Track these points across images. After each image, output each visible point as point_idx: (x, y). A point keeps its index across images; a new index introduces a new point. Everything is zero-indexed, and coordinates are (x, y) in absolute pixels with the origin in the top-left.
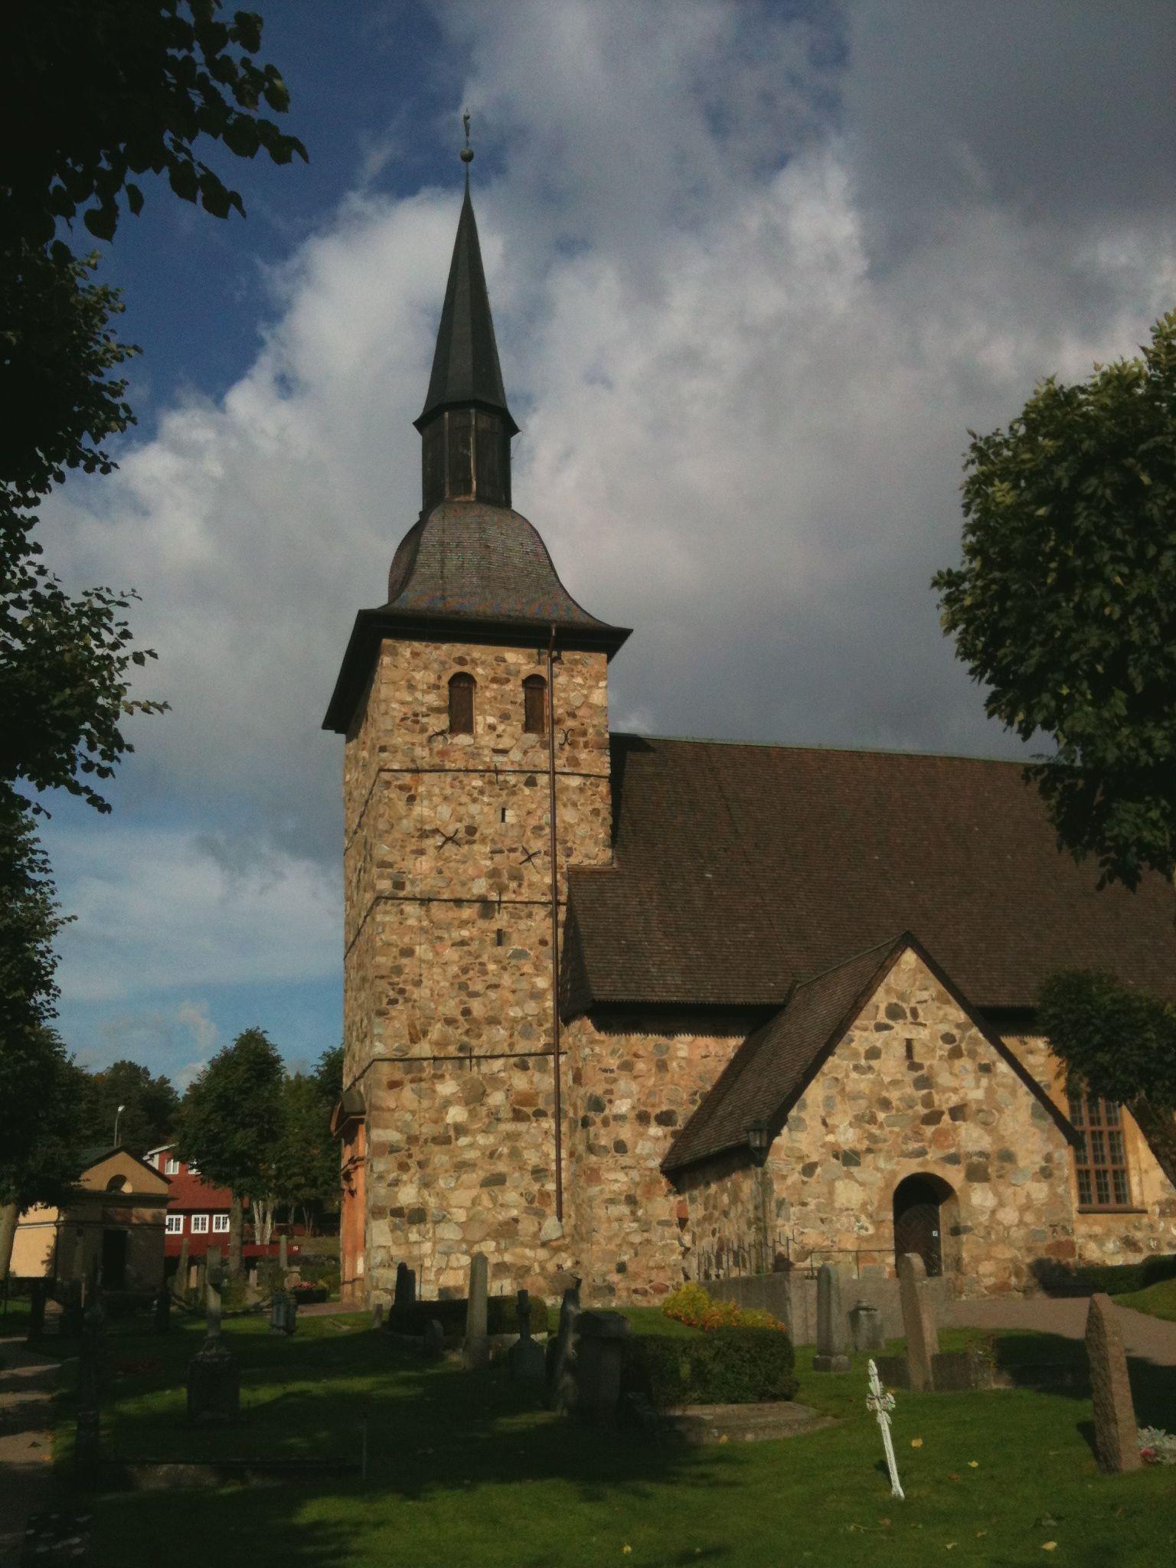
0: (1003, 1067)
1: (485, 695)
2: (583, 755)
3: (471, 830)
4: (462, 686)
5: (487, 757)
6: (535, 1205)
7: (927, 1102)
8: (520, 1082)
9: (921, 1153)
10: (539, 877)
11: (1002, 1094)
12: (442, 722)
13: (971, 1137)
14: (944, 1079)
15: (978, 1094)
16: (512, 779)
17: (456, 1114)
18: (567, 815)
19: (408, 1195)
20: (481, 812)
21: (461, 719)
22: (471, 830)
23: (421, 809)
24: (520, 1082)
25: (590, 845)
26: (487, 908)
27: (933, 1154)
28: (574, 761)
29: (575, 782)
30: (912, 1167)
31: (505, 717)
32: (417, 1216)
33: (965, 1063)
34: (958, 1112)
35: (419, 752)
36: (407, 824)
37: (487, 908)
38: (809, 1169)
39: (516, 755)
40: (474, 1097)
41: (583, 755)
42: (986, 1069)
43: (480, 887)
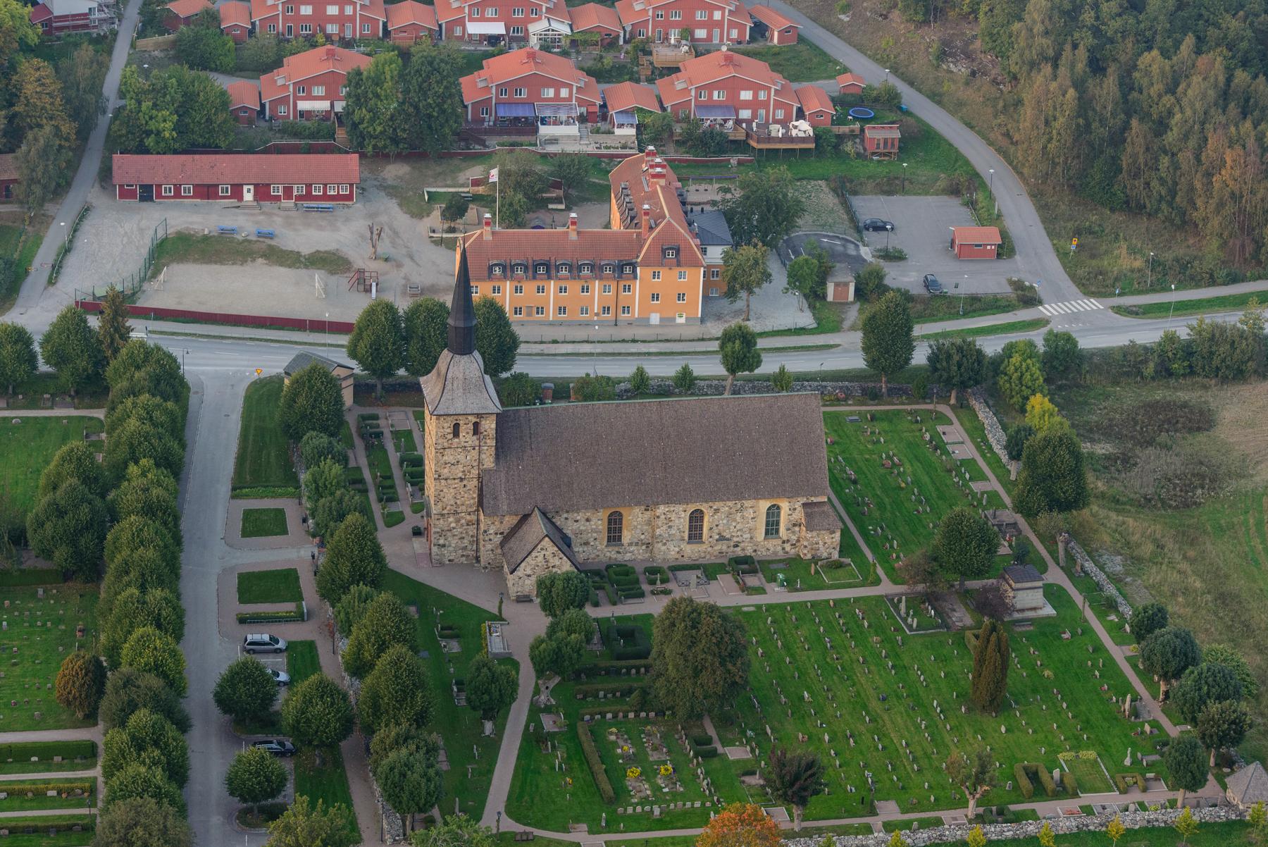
1: (462, 428)
6: (471, 543)
8: (468, 517)
10: (475, 472)
17: (453, 525)
18: (483, 456)
19: (441, 542)
20: (461, 457)
21: (456, 433)
23: (446, 458)
24: (468, 517)
25: (489, 462)
26: (462, 480)
32: (444, 546)
37: (462, 480)
40: (458, 521)
43: (460, 475)
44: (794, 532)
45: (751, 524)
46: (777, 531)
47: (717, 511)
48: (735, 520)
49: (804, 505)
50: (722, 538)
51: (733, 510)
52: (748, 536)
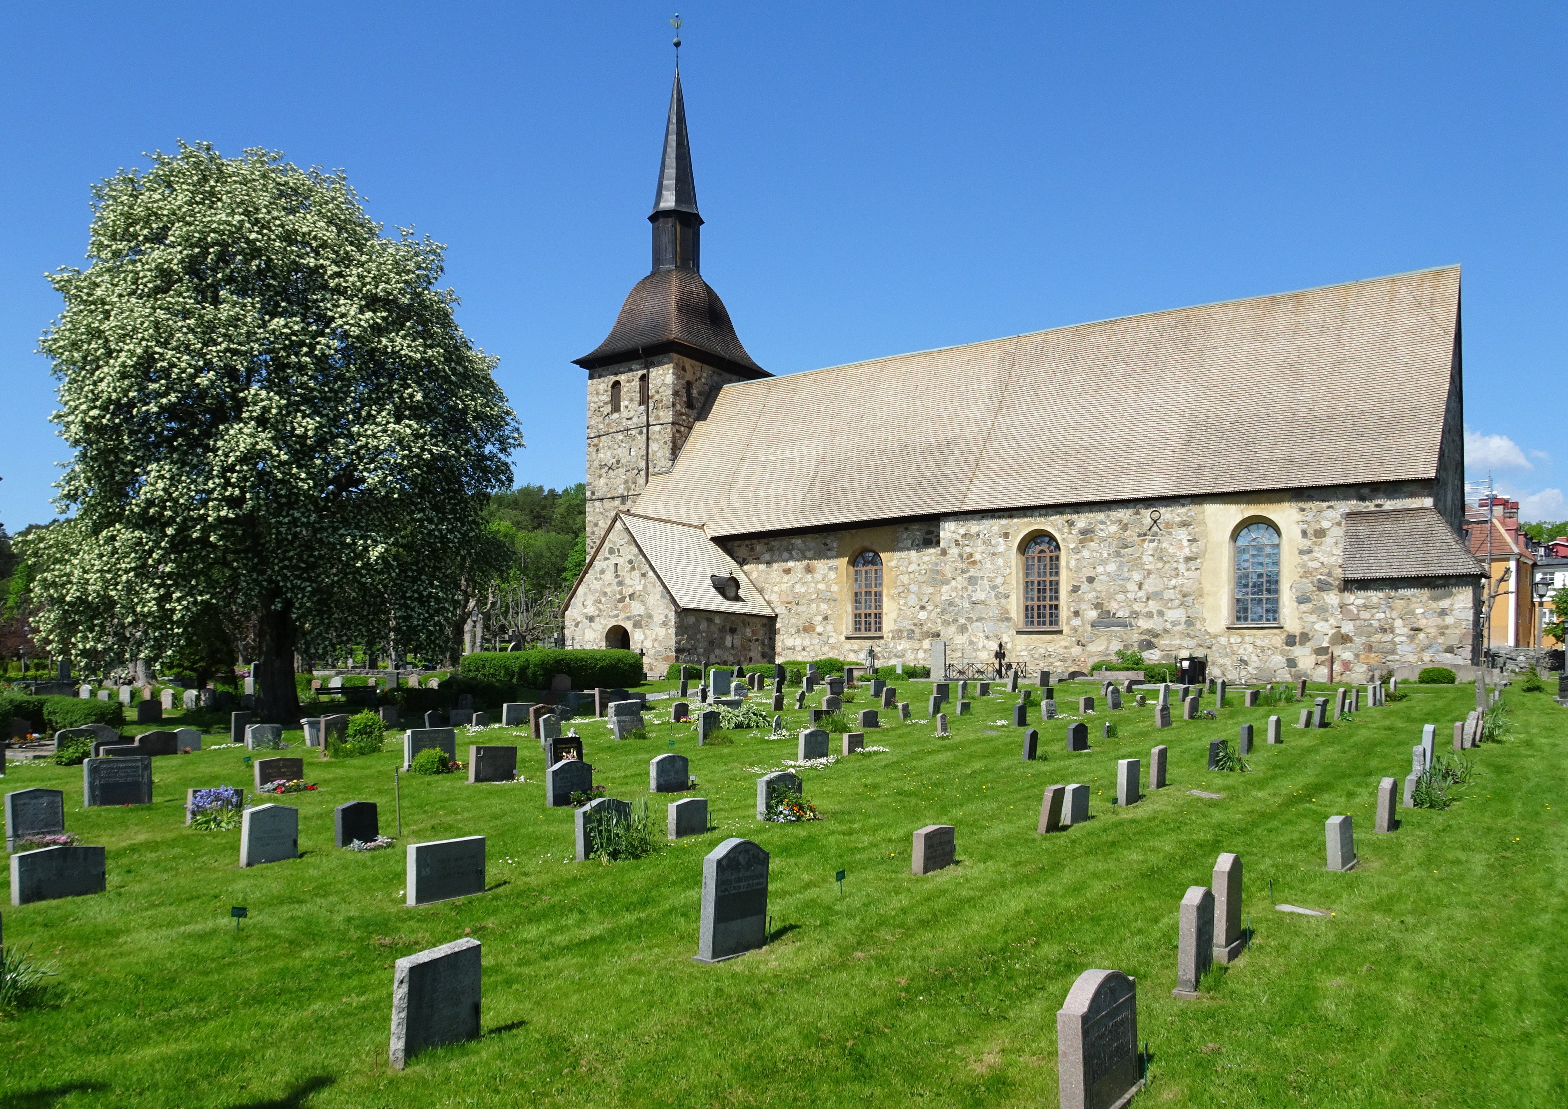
0: (651, 573)
1: (625, 388)
2: (661, 413)
3: (618, 462)
4: (617, 384)
5: (625, 423)
7: (621, 593)
9: (617, 616)
11: (650, 587)
12: (608, 408)
13: (636, 608)
14: (628, 581)
15: (640, 588)
16: (633, 432)
18: (654, 446)
20: (621, 452)
22: (618, 462)
23: (601, 455)
27: (622, 615)
28: (658, 418)
29: (657, 428)
30: (613, 623)
31: (631, 400)
33: (636, 573)
34: (631, 596)
35: (601, 426)
36: (596, 464)
38: (577, 625)
39: (635, 420)
41: (661, 413)
42: (644, 575)
44: (1322, 611)
45: (1186, 579)
46: (1273, 610)
47: (1087, 534)
48: (1137, 563)
49: (1350, 515)
50: (1106, 620)
51: (1131, 534)
52: (1176, 614)
